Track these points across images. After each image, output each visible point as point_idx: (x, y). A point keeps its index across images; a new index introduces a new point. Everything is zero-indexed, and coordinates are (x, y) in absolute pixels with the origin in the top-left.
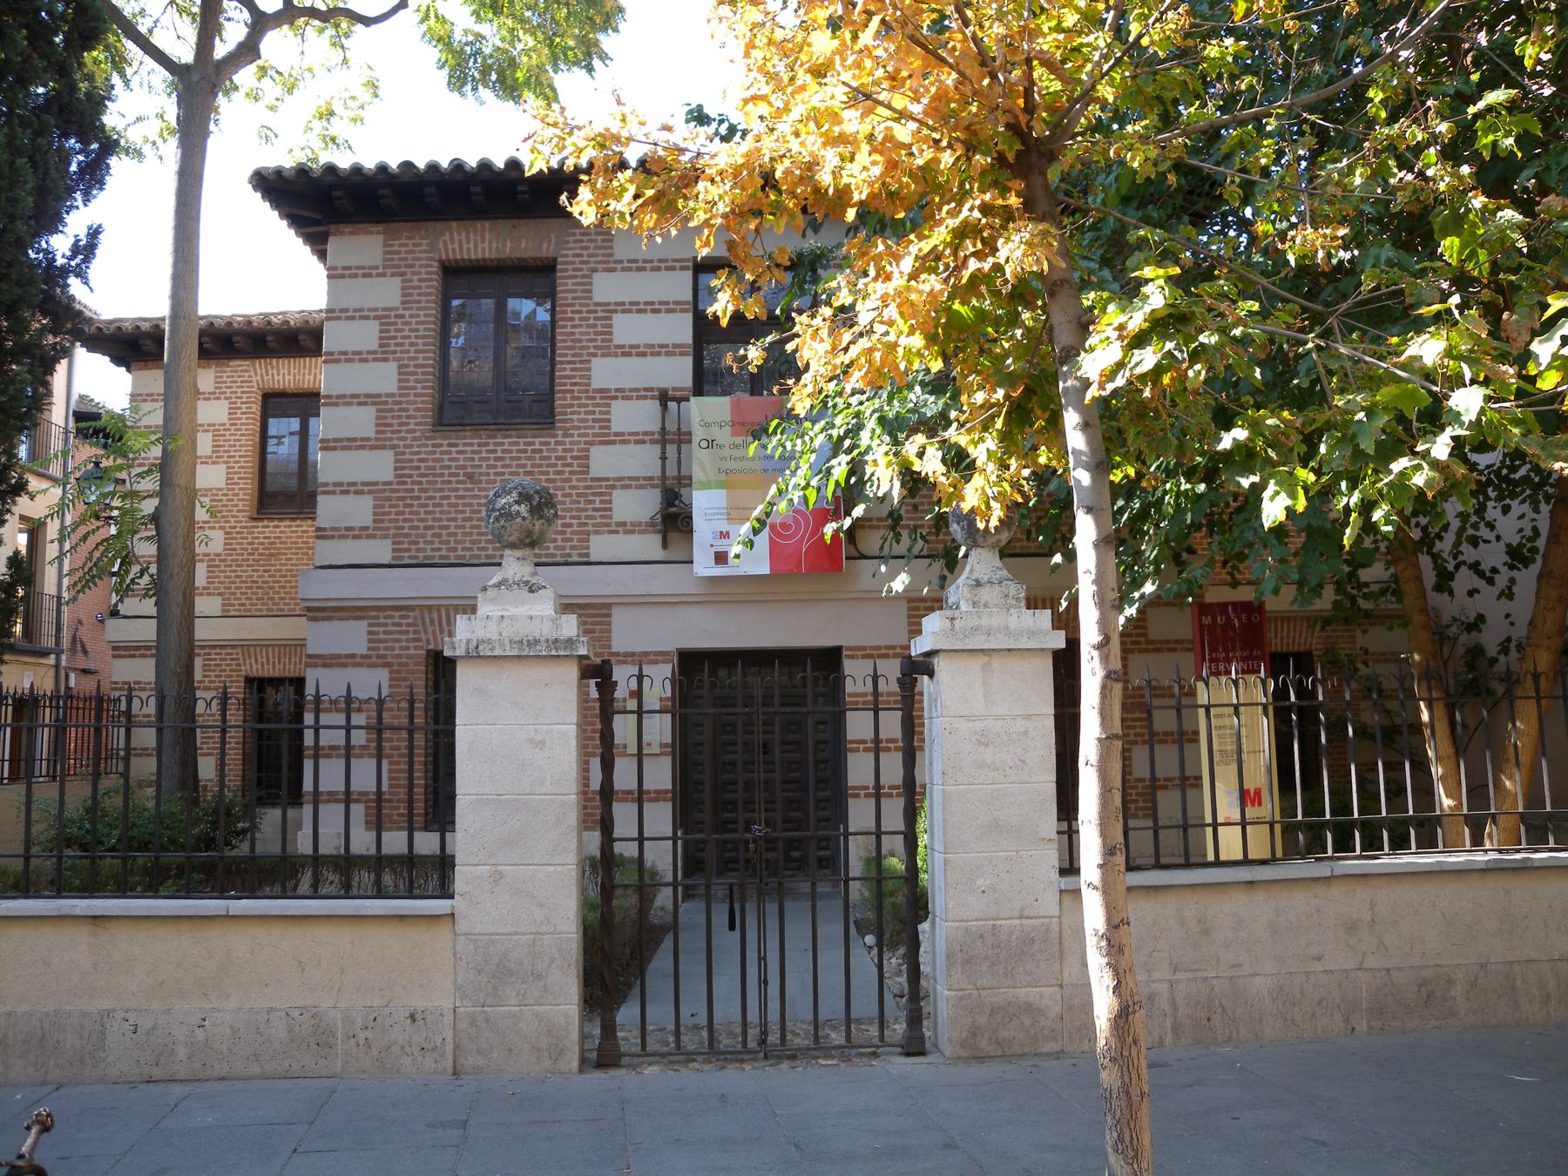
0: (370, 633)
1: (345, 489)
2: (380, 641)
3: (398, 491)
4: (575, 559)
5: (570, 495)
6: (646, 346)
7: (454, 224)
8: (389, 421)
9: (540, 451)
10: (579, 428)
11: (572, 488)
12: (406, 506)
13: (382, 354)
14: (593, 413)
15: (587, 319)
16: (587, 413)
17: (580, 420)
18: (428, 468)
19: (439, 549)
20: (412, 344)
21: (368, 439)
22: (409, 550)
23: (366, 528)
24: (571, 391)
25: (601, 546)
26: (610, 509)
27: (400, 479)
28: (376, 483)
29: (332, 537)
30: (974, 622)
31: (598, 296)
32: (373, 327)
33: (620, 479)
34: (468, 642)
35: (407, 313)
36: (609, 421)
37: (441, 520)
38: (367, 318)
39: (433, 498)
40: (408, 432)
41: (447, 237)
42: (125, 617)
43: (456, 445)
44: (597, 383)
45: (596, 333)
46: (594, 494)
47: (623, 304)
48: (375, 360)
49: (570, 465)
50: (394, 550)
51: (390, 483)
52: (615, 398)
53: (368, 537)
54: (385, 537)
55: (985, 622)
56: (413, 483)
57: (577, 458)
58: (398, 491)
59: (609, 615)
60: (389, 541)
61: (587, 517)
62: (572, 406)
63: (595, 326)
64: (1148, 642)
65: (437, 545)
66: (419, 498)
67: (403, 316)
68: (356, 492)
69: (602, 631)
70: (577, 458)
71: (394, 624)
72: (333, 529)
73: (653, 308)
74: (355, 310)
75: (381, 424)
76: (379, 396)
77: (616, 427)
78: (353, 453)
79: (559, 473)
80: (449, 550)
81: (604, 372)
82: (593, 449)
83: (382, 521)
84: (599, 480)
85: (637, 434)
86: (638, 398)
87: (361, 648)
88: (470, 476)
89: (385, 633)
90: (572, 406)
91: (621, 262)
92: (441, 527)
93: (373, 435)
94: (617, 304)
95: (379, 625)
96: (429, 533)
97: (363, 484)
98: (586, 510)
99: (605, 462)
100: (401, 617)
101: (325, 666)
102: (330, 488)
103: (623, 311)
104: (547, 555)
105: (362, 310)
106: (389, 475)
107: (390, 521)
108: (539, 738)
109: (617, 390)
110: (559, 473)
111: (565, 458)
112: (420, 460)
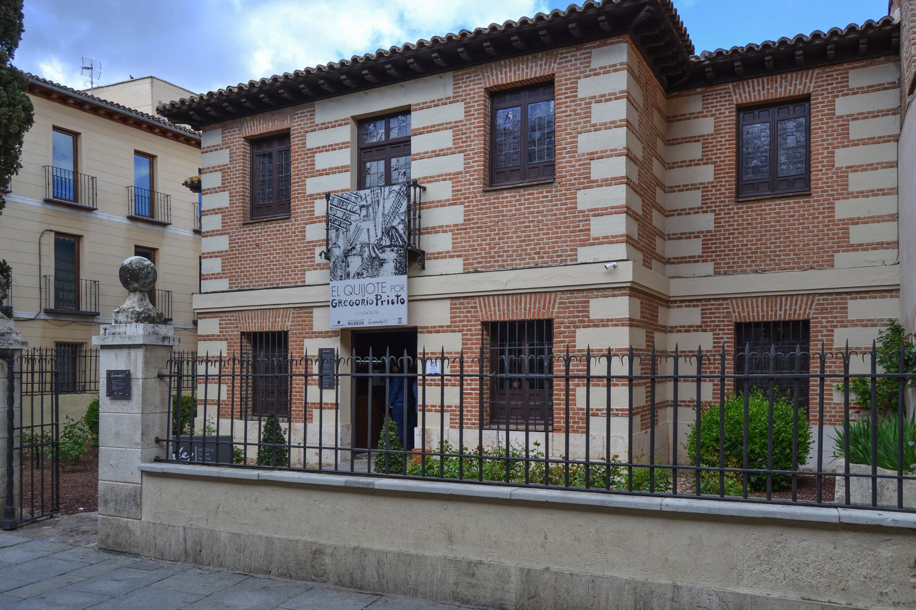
4: (299, 284)
6: (330, 169)
13: (223, 189)
44: (308, 192)
51: (227, 251)
52: (316, 199)
57: (301, 232)
64: (592, 321)
70: (301, 232)
73: (332, 148)
79: (293, 240)
82: (307, 226)
88: (257, 245)
103: (320, 152)
106: (227, 248)
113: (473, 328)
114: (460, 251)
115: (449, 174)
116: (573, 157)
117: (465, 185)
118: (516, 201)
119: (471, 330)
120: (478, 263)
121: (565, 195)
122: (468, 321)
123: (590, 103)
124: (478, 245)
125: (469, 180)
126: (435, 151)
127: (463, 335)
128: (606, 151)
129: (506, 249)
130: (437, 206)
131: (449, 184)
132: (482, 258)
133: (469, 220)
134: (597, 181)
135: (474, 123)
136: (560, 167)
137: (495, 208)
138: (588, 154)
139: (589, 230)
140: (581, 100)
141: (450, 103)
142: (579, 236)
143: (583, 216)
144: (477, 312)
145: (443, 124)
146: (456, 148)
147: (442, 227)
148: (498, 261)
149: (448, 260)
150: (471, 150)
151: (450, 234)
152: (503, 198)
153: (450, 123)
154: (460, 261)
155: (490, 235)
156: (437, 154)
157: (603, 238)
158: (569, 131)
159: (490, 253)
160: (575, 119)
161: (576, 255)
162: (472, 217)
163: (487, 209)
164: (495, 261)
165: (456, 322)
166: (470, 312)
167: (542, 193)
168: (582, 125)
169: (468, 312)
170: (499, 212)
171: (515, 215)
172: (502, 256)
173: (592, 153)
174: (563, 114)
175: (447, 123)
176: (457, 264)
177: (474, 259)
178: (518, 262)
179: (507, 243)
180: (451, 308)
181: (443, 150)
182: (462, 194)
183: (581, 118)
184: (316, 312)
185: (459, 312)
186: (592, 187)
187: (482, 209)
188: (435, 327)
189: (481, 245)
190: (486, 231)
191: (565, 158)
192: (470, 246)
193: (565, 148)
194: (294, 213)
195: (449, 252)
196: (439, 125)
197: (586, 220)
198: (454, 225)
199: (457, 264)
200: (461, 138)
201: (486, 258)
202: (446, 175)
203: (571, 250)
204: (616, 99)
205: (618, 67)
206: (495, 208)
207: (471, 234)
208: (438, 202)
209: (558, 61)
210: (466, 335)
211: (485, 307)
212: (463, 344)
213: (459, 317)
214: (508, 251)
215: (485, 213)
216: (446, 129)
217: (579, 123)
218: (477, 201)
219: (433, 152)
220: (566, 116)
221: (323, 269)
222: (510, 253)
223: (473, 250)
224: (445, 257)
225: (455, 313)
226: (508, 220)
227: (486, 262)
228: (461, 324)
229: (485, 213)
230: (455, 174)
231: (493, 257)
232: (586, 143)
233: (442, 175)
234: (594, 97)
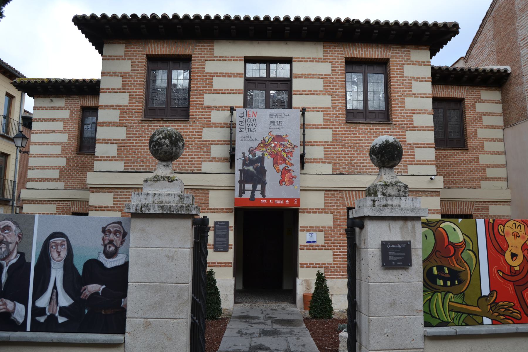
0: (114, 198)
1: (107, 141)
2: (118, 201)
3: (128, 143)
4: (196, 171)
5: (194, 147)
6: (225, 90)
7: (152, 41)
8: (125, 116)
9: (184, 129)
10: (199, 121)
11: (196, 144)
12: (130, 149)
13: (123, 90)
14: (204, 115)
15: (203, 79)
16: (202, 115)
17: (199, 118)
18: (139, 134)
19: (143, 166)
20: (135, 86)
21: (117, 123)
22: (131, 166)
23: (114, 157)
24: (196, 107)
25: (206, 166)
26: (210, 152)
27: (129, 138)
28: (119, 140)
29: (101, 160)
30: (385, 202)
31: (208, 70)
32: (120, 79)
33: (214, 141)
34: (137, 206)
35: (133, 74)
36: (210, 118)
37: (144, 155)
38: (118, 76)
39: (141, 146)
40: (132, 120)
41: (150, 46)
42: (27, 189)
43: (151, 126)
44: (206, 104)
45: (206, 84)
46: (204, 146)
47: (217, 73)
48: (120, 92)
49: (195, 135)
50: (125, 166)
51: (124, 140)
52: (213, 110)
53: (115, 160)
54: (122, 161)
55: (390, 202)
56: (133, 140)
57: (198, 132)
58: (128, 143)
59: (208, 194)
60: (124, 162)
61: (201, 155)
62: (196, 112)
63: (206, 82)
65: (142, 164)
66: (136, 146)
67: (131, 75)
68: (111, 143)
69: (205, 200)
70: (198, 132)
71: (124, 195)
72: (101, 157)
73: (228, 75)
74: (113, 73)
75: (122, 117)
76: (121, 106)
77: (213, 121)
78: (110, 127)
79: (190, 138)
80: (146, 166)
81: (209, 100)
82: (204, 129)
83: (121, 154)
84: (206, 141)
85: (221, 123)
86: (222, 110)
87: (110, 203)
89: (120, 198)
90: (196, 112)
91: (217, 57)
92: (144, 158)
93: (118, 121)
94: (214, 73)
95: (118, 195)
96: (139, 159)
97: (114, 140)
98: (200, 153)
99: (208, 134)
100: (127, 192)
101: (96, 210)
102: (101, 141)
103: (217, 76)
104: (185, 170)
105: (116, 73)
106: (124, 137)
107: (124, 154)
108: (170, 255)
109: (214, 107)
110: (190, 138)
111: (193, 132)
112: (136, 131)
113: (341, 211)
114: (330, 160)
115: (321, 108)
116: (403, 110)
117: (333, 117)
118: (368, 132)
119: (340, 213)
120: (343, 168)
121: (399, 132)
122: (338, 206)
123: (411, 80)
124: (343, 157)
125: (336, 114)
126: (311, 91)
127: (334, 216)
128: (422, 110)
129: (362, 161)
130: (313, 128)
131: (321, 114)
132: (346, 165)
133: (336, 140)
134: (417, 127)
135: (339, 78)
136: (395, 115)
137: (354, 134)
138: (411, 110)
139: (414, 155)
140: (406, 77)
141: (322, 62)
142: (408, 158)
143: (410, 146)
144: (344, 200)
145: (316, 74)
146: (326, 92)
147: (316, 142)
148: (357, 169)
149: (321, 164)
150: (336, 95)
151: (323, 147)
152: (359, 129)
153: (322, 75)
154: (330, 166)
155: (351, 151)
156: (312, 93)
157: (423, 161)
158: (399, 94)
159: (351, 163)
160: (403, 88)
161: (407, 169)
162: (338, 138)
163: (348, 134)
164: (355, 169)
165: (328, 207)
166: (339, 200)
167: (385, 129)
168: (407, 92)
169: (337, 200)
170: (356, 137)
171: (368, 140)
172: (360, 166)
173: (414, 110)
174: (396, 84)
175: (319, 75)
176: (328, 168)
177: (340, 166)
178: (370, 170)
179: (363, 157)
180: (325, 197)
181: (317, 91)
182: (331, 122)
183: (406, 88)
184: (212, 193)
185: (331, 200)
186: (414, 130)
187: (345, 134)
188: (313, 209)
189: (345, 157)
190: (348, 148)
191: (398, 110)
192: (337, 157)
193: (398, 104)
194: (193, 118)
195: (322, 159)
196: (313, 75)
197: (412, 149)
198: (325, 142)
199: (328, 168)
200: (329, 86)
201: (348, 165)
202: (319, 108)
203: (404, 166)
204: (426, 81)
205: (426, 63)
206: (354, 134)
207: (338, 149)
208: (313, 125)
209: (391, 51)
210: (337, 215)
211: (350, 198)
212: (334, 222)
213: (331, 203)
214: (363, 163)
215: (347, 137)
216: (319, 78)
217: (405, 91)
218: (341, 128)
219: (309, 91)
220: (398, 85)
221: (218, 162)
222: (365, 164)
223: (339, 160)
224: (319, 162)
225: (328, 200)
226: (362, 143)
227: (349, 168)
228: (332, 208)
229: (347, 137)
230: (326, 108)
231: (354, 166)
232: (410, 103)
233: (316, 108)
234: (414, 78)
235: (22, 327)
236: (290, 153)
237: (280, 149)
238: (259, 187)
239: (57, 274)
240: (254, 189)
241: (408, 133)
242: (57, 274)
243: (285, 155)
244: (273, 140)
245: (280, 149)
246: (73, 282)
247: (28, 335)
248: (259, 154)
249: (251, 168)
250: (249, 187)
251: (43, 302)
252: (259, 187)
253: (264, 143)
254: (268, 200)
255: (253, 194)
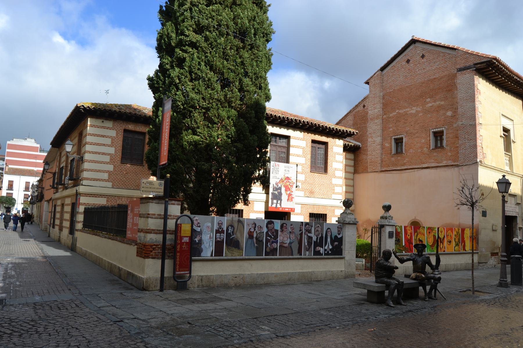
235: (322, 255)
236: (292, 186)
237: (288, 184)
238: (279, 202)
239: (329, 240)
240: (277, 203)
241: (333, 179)
242: (329, 240)
243: (290, 187)
244: (286, 179)
245: (288, 184)
246: (332, 242)
247: (323, 256)
248: (280, 185)
249: (276, 192)
250: (275, 201)
251: (326, 248)
252: (279, 202)
253: (282, 180)
254: (283, 208)
255: (276, 205)
